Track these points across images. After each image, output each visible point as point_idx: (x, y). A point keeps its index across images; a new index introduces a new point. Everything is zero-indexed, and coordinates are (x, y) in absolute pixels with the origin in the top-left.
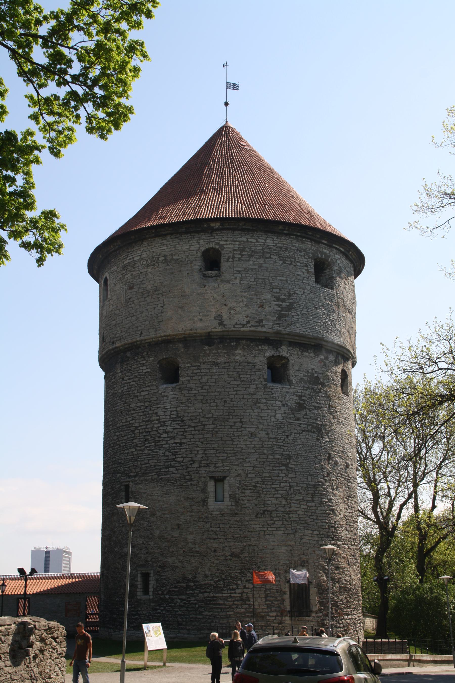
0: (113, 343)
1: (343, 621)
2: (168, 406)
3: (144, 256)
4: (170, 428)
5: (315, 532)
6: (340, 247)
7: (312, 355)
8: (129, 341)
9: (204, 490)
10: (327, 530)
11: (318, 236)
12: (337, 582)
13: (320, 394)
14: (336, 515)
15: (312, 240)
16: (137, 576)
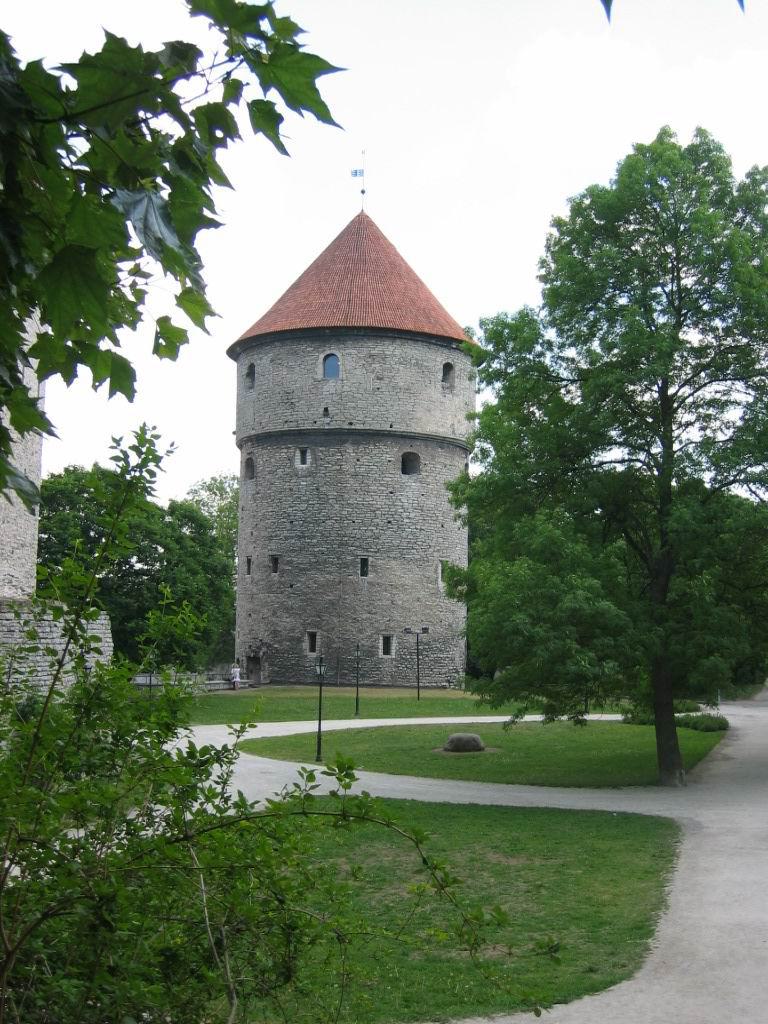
0: (351, 424)
2: (410, 494)
3: (397, 352)
4: (412, 515)
8: (378, 427)
9: (436, 571)
16: (378, 639)
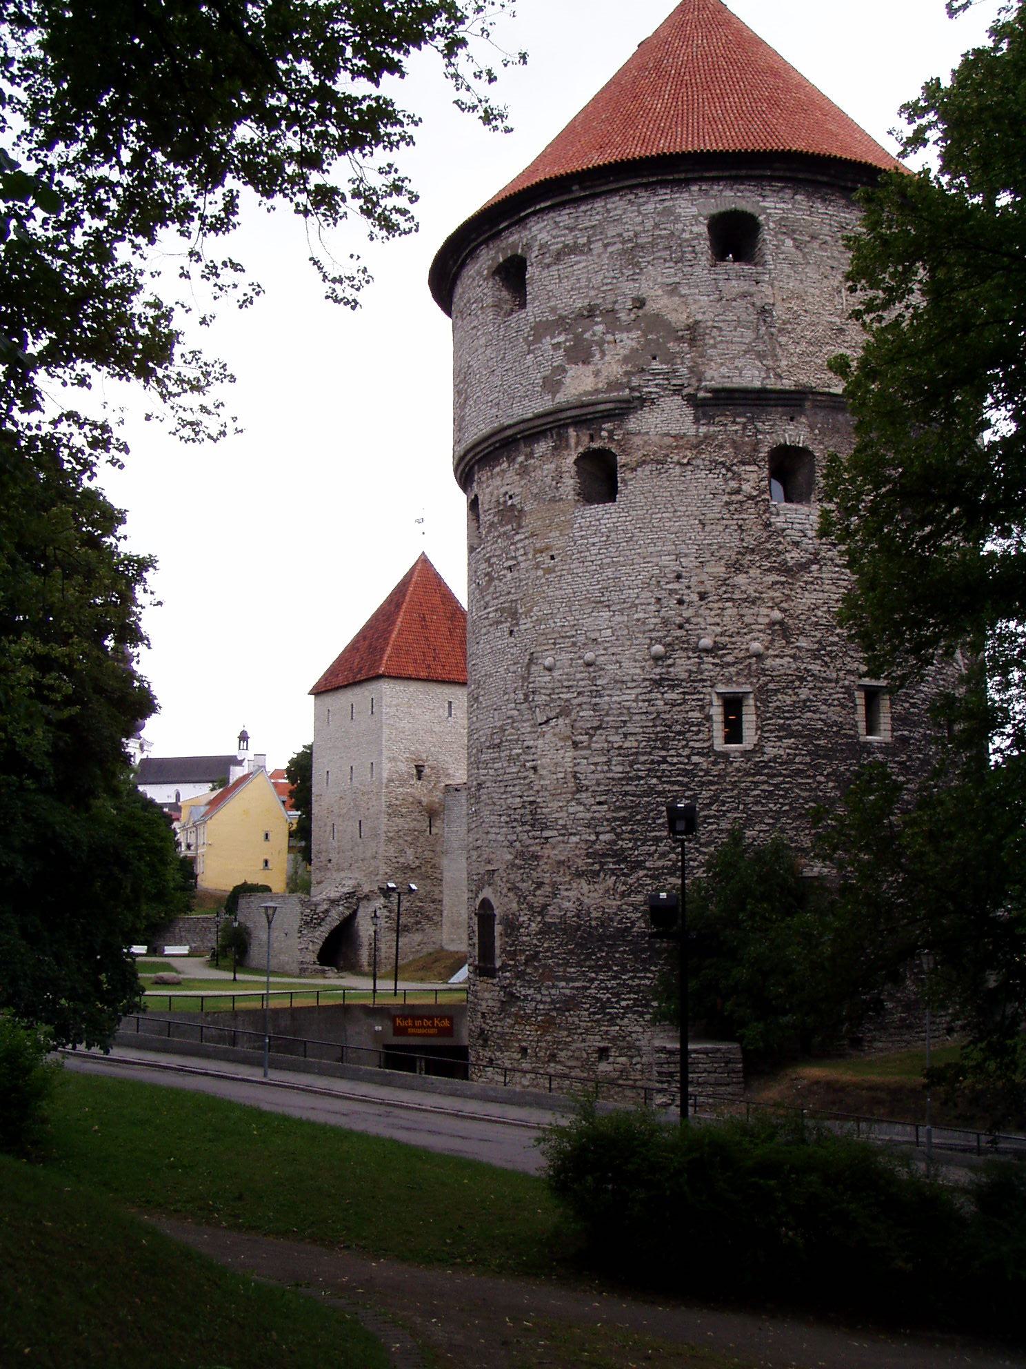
1: (553, 991)
5: (504, 819)
6: (535, 204)
7: (505, 465)
10: (522, 811)
11: (487, 227)
12: (540, 913)
13: (517, 538)
14: (541, 777)
15: (486, 242)
